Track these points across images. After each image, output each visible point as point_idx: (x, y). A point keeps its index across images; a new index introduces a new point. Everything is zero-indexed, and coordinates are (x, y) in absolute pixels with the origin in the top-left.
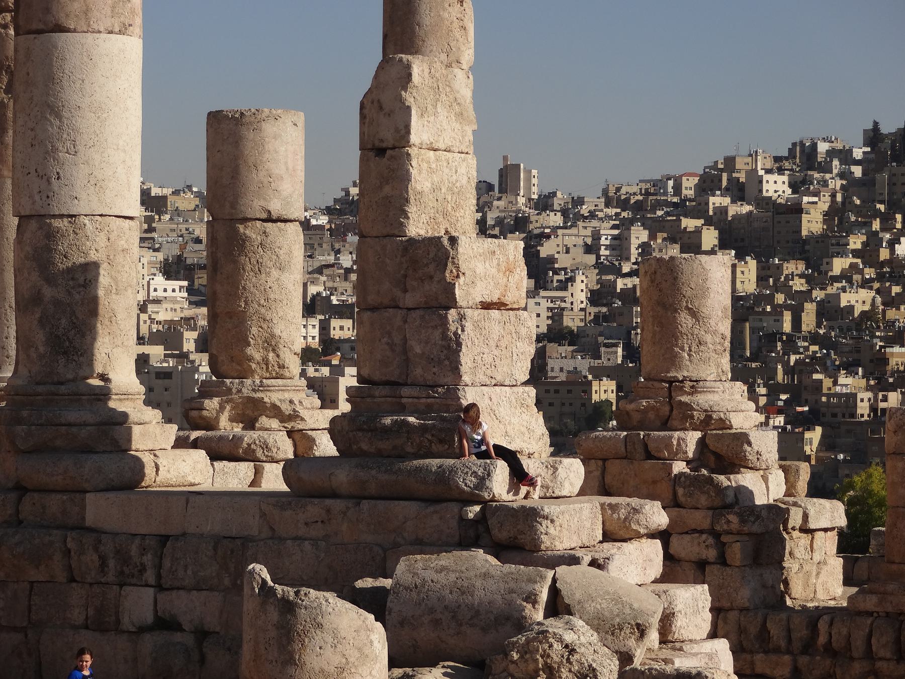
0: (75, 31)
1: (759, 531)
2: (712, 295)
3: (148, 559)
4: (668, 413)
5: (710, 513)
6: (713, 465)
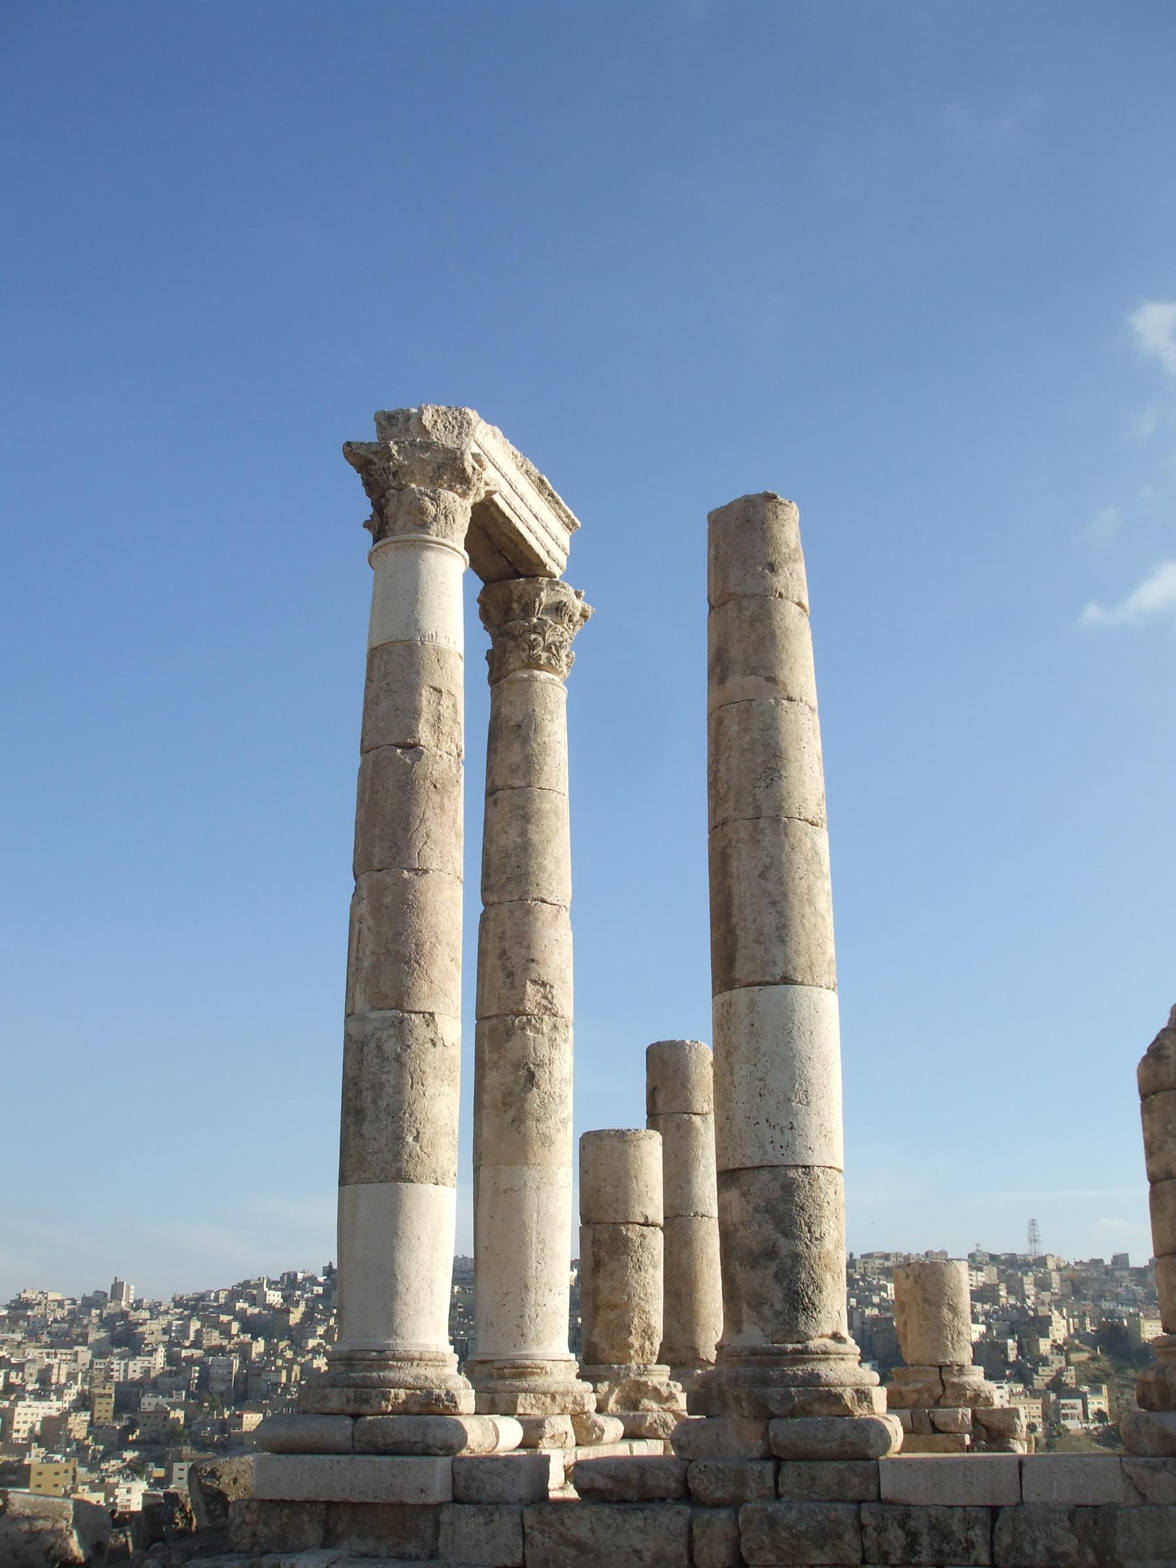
0: (802, 984)
3: (977, 1534)
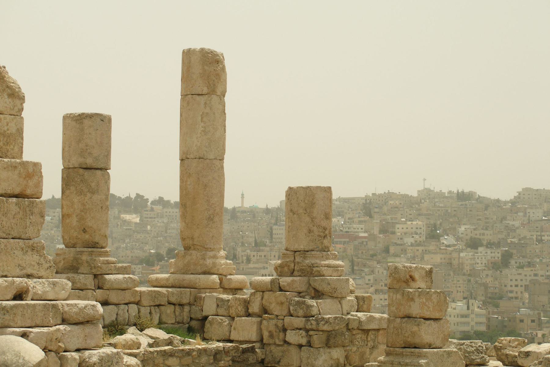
1: (328, 330)
2: (317, 207)
4: (293, 268)
5: (304, 319)
6: (313, 295)
